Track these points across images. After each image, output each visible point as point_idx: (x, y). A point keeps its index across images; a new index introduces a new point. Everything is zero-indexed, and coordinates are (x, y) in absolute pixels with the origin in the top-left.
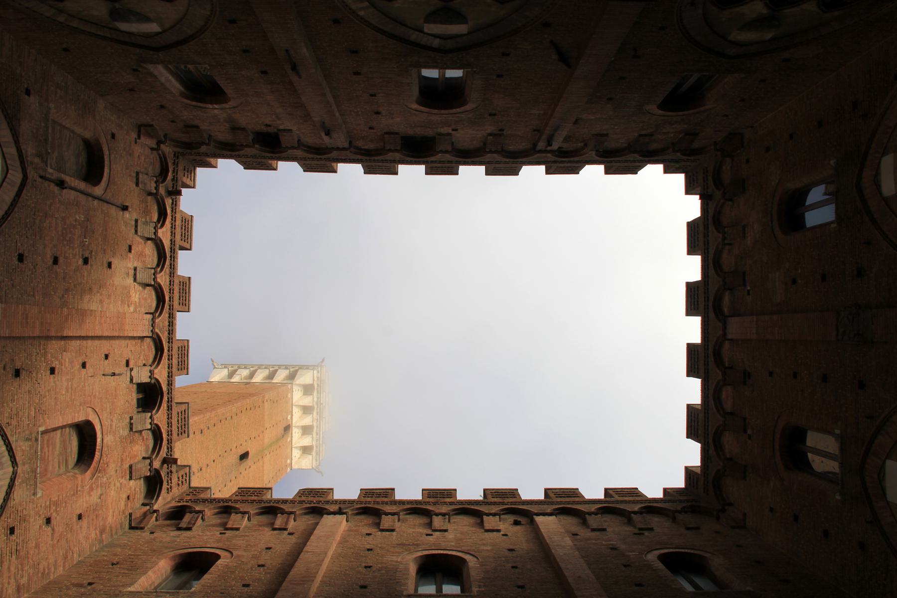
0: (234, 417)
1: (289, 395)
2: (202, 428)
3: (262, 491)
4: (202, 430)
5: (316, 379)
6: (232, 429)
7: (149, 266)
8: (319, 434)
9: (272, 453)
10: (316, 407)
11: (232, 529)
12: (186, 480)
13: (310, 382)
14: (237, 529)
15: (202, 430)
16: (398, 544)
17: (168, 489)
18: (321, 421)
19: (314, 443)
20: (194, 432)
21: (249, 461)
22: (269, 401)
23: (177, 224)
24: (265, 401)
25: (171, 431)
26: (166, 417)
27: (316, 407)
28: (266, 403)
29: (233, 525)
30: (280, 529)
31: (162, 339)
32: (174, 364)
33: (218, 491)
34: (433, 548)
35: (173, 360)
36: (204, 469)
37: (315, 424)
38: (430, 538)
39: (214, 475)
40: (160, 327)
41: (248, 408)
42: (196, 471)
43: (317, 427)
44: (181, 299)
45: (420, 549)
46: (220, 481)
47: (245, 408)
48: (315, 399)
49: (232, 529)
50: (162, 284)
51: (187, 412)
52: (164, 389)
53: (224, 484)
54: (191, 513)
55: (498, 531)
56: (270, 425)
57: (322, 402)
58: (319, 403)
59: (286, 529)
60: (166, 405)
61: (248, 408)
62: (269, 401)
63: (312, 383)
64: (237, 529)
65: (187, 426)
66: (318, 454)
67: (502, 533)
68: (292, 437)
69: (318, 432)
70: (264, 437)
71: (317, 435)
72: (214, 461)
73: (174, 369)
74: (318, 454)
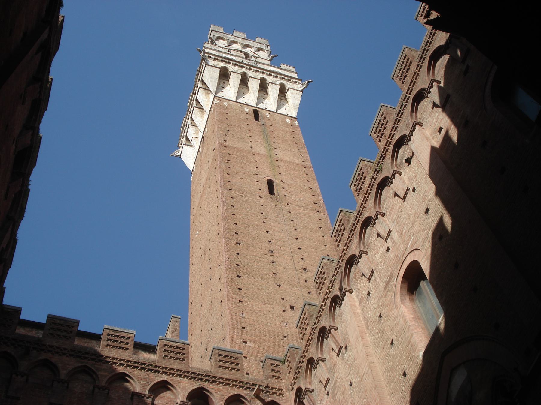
0: (234, 193)
1: (226, 104)
2: (235, 242)
3: (305, 313)
4: (237, 243)
5: (216, 63)
6: (243, 199)
7: (91, 388)
8: (271, 73)
9: (276, 145)
10: (244, 70)
11: (327, 383)
12: (277, 365)
13: (218, 71)
14: (328, 380)
15: (237, 243)
16: (385, 289)
17: (280, 394)
18: (260, 66)
19: (279, 81)
20: (237, 254)
21: (277, 182)
22: (226, 138)
23: (55, 344)
24: (225, 144)
25: (233, 381)
26: (220, 387)
27: (244, 70)
28: (228, 143)
29: (324, 379)
30: (340, 351)
31: (155, 382)
32: (179, 367)
33: (295, 232)
34: (399, 267)
35: (175, 367)
36: (272, 247)
37: (260, 76)
38: (391, 254)
39: (279, 234)
40: (145, 384)
41: (227, 171)
42: (271, 258)
43: (263, 73)
44: (122, 345)
45: (395, 280)
46: (287, 227)
47: (227, 175)
48: (236, 68)
49: (327, 383)
50: (108, 377)
51: (221, 353)
52: (198, 386)
53: (291, 222)
54: (304, 398)
55: (408, 190)
56: (249, 141)
57: (240, 60)
58: (241, 65)
59: (341, 348)
60: (211, 386)
61: (227, 171)
62: (226, 138)
63: (219, 69)
64: (328, 380)
65: (233, 355)
66: (290, 79)
67: (411, 189)
68: (266, 110)
69: (269, 73)
70: (258, 154)
71: (270, 75)
72: (267, 232)
73: (183, 367)
74: (290, 79)
